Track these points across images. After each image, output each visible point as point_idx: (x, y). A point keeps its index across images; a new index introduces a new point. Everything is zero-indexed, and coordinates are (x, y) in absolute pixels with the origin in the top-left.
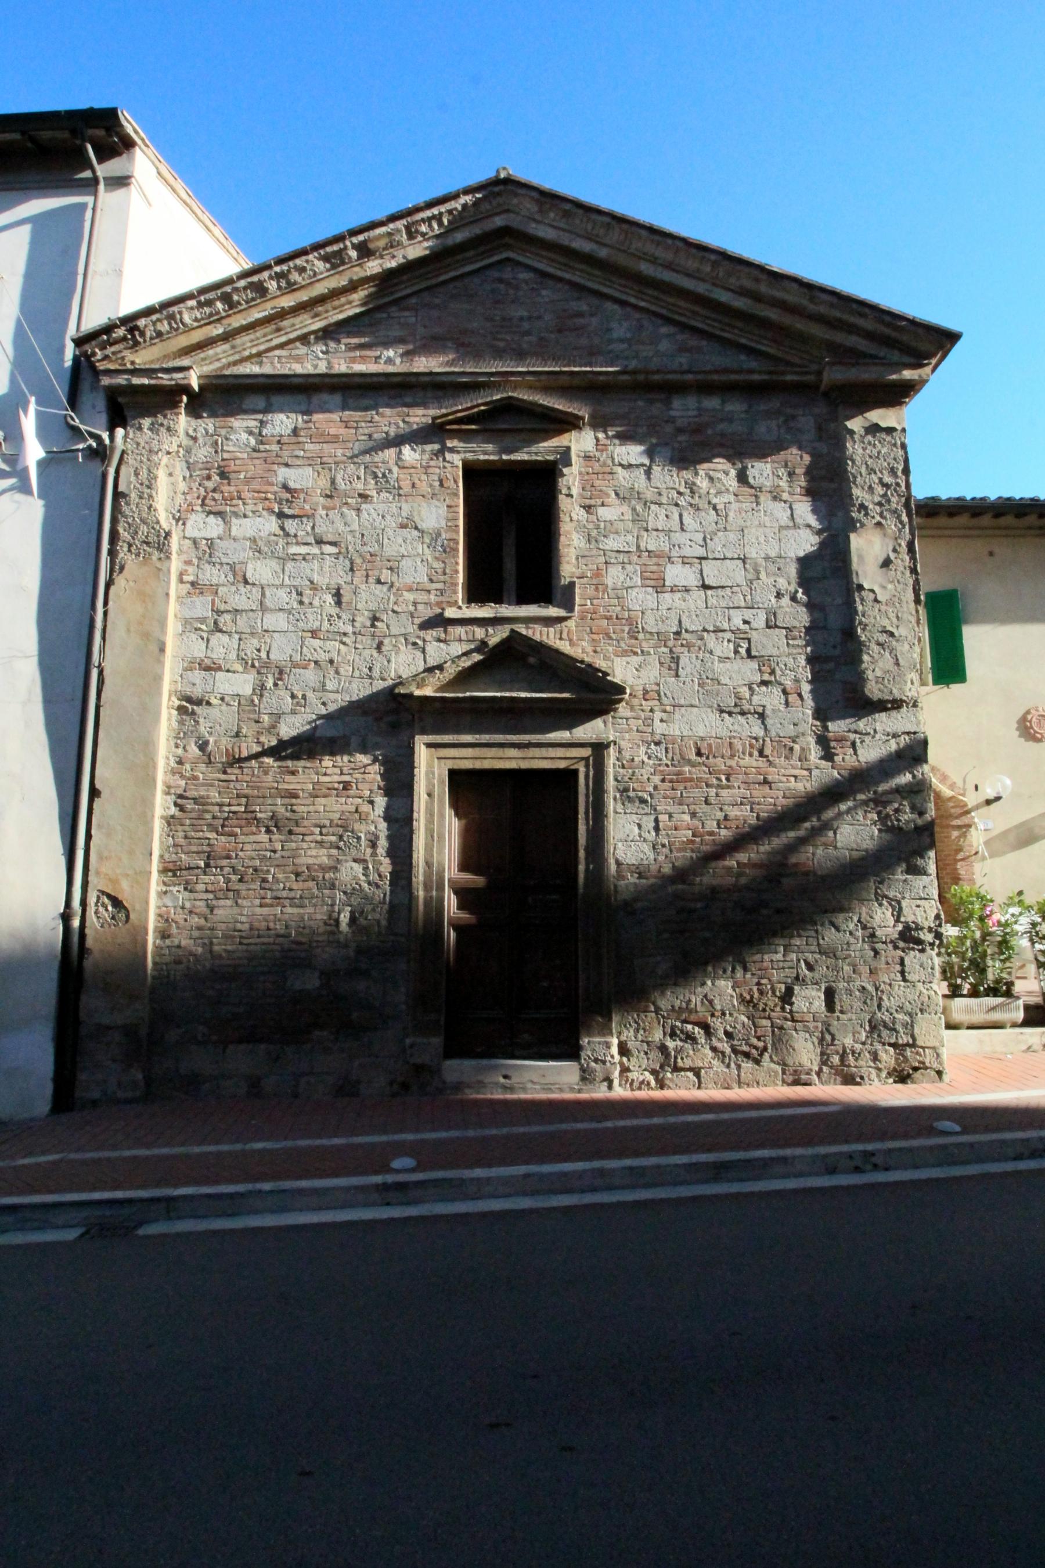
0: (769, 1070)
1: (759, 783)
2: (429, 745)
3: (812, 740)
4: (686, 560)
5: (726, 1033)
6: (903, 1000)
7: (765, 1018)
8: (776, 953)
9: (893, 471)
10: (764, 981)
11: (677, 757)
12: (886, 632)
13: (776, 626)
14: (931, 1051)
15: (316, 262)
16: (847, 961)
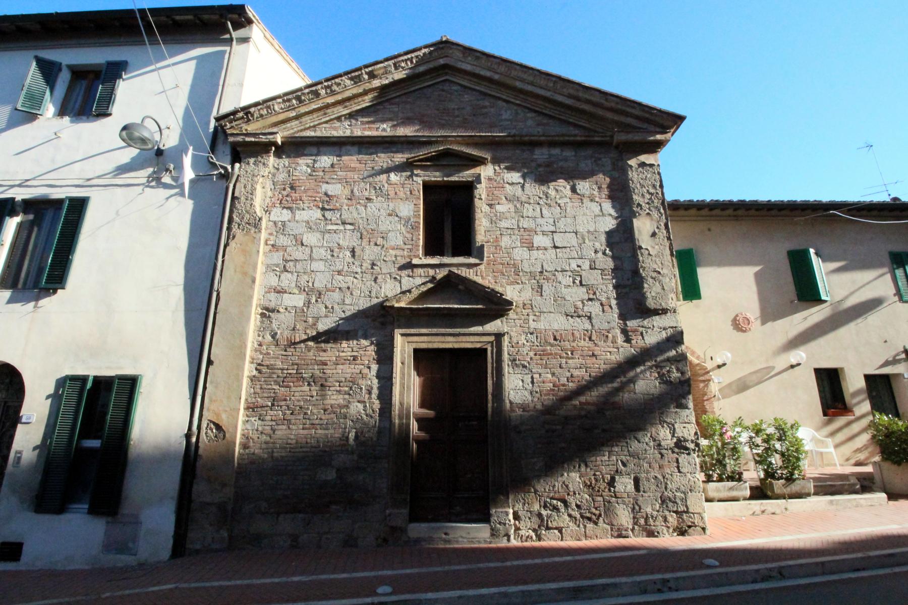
2: (402, 335)
3: (618, 331)
5: (577, 506)
9: (654, 186)
10: (598, 473)
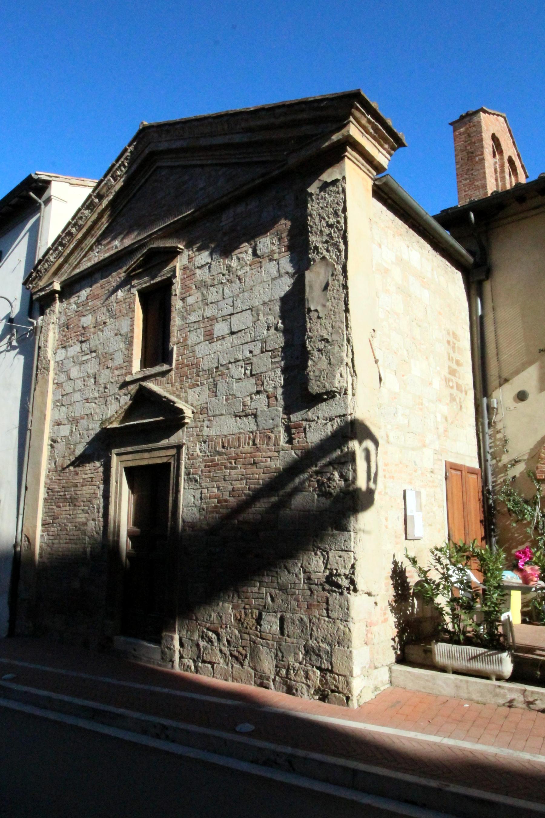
0: (248, 673)
1: (251, 464)
2: (117, 455)
3: (282, 430)
4: (224, 318)
5: (228, 641)
6: (326, 633)
7: (246, 633)
8: (255, 586)
9: (336, 214)
10: (247, 607)
11: (213, 450)
12: (323, 340)
13: (267, 351)
14: (343, 678)
15: (85, 212)
16: (294, 597)
